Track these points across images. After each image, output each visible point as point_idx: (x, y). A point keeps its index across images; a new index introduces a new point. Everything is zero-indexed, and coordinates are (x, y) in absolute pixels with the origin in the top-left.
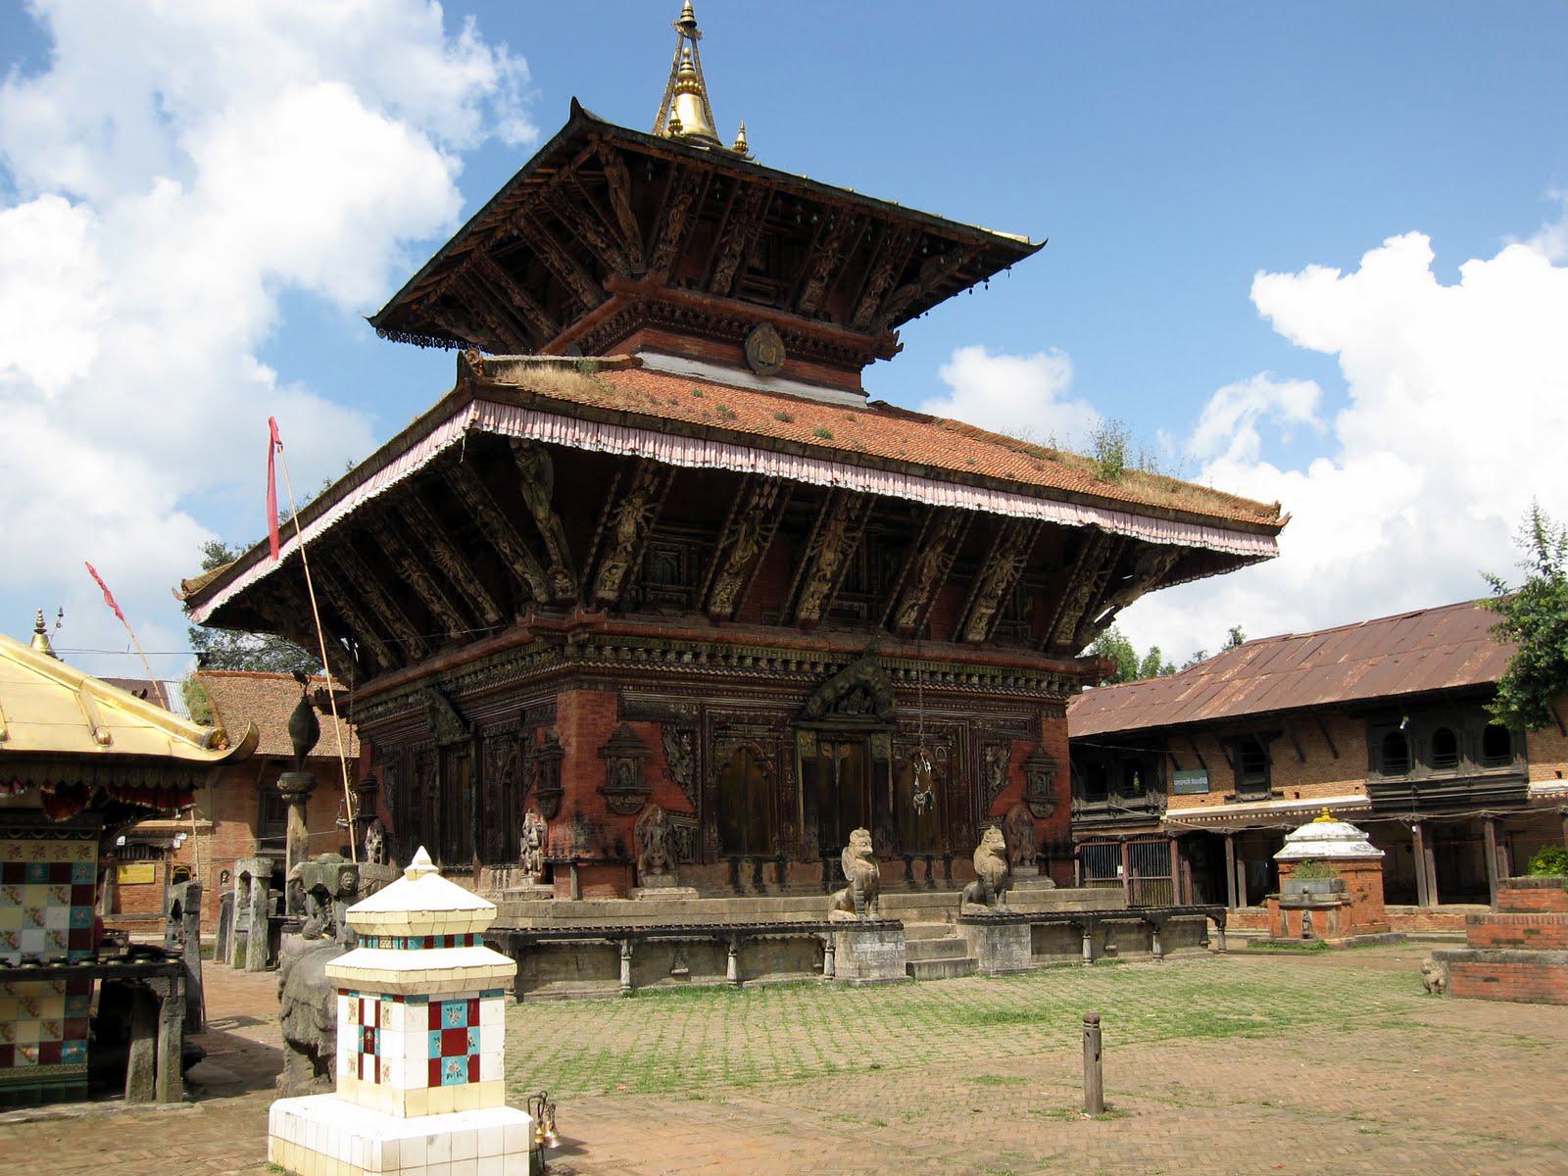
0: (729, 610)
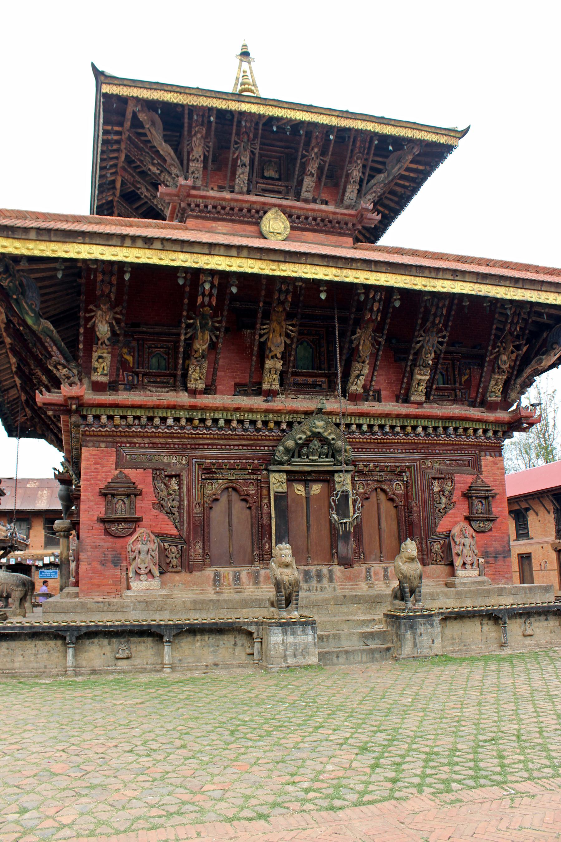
0: (201, 386)
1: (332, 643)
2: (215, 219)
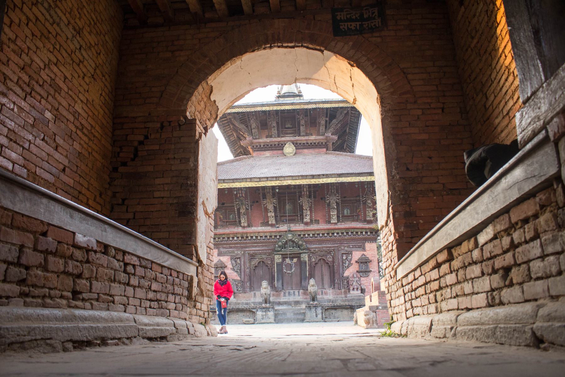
0: (246, 225)
1: (283, 316)
2: (265, 150)
